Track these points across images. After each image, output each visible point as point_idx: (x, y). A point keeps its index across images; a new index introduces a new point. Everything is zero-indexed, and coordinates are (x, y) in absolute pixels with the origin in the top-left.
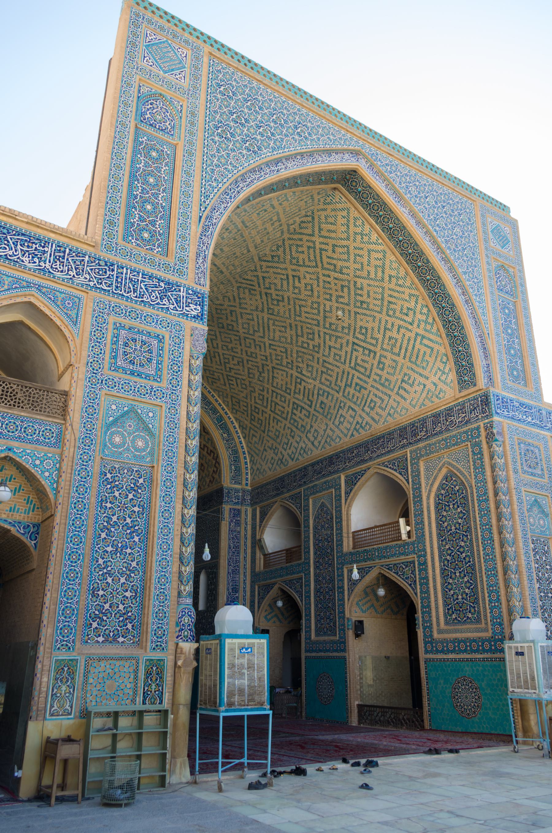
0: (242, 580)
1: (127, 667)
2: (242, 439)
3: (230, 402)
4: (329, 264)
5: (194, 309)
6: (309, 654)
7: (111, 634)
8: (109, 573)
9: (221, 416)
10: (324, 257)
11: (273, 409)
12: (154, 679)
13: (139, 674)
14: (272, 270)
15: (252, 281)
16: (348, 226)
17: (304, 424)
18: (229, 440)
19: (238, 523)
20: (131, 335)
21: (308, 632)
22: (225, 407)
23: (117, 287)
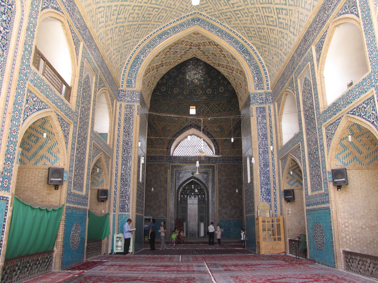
0: (270, 158)
2: (261, 57)
3: (245, 33)
6: (308, 208)
11: (267, 23)
17: (287, 22)
18: (250, 60)
19: (264, 117)
21: (306, 189)
22: (244, 38)
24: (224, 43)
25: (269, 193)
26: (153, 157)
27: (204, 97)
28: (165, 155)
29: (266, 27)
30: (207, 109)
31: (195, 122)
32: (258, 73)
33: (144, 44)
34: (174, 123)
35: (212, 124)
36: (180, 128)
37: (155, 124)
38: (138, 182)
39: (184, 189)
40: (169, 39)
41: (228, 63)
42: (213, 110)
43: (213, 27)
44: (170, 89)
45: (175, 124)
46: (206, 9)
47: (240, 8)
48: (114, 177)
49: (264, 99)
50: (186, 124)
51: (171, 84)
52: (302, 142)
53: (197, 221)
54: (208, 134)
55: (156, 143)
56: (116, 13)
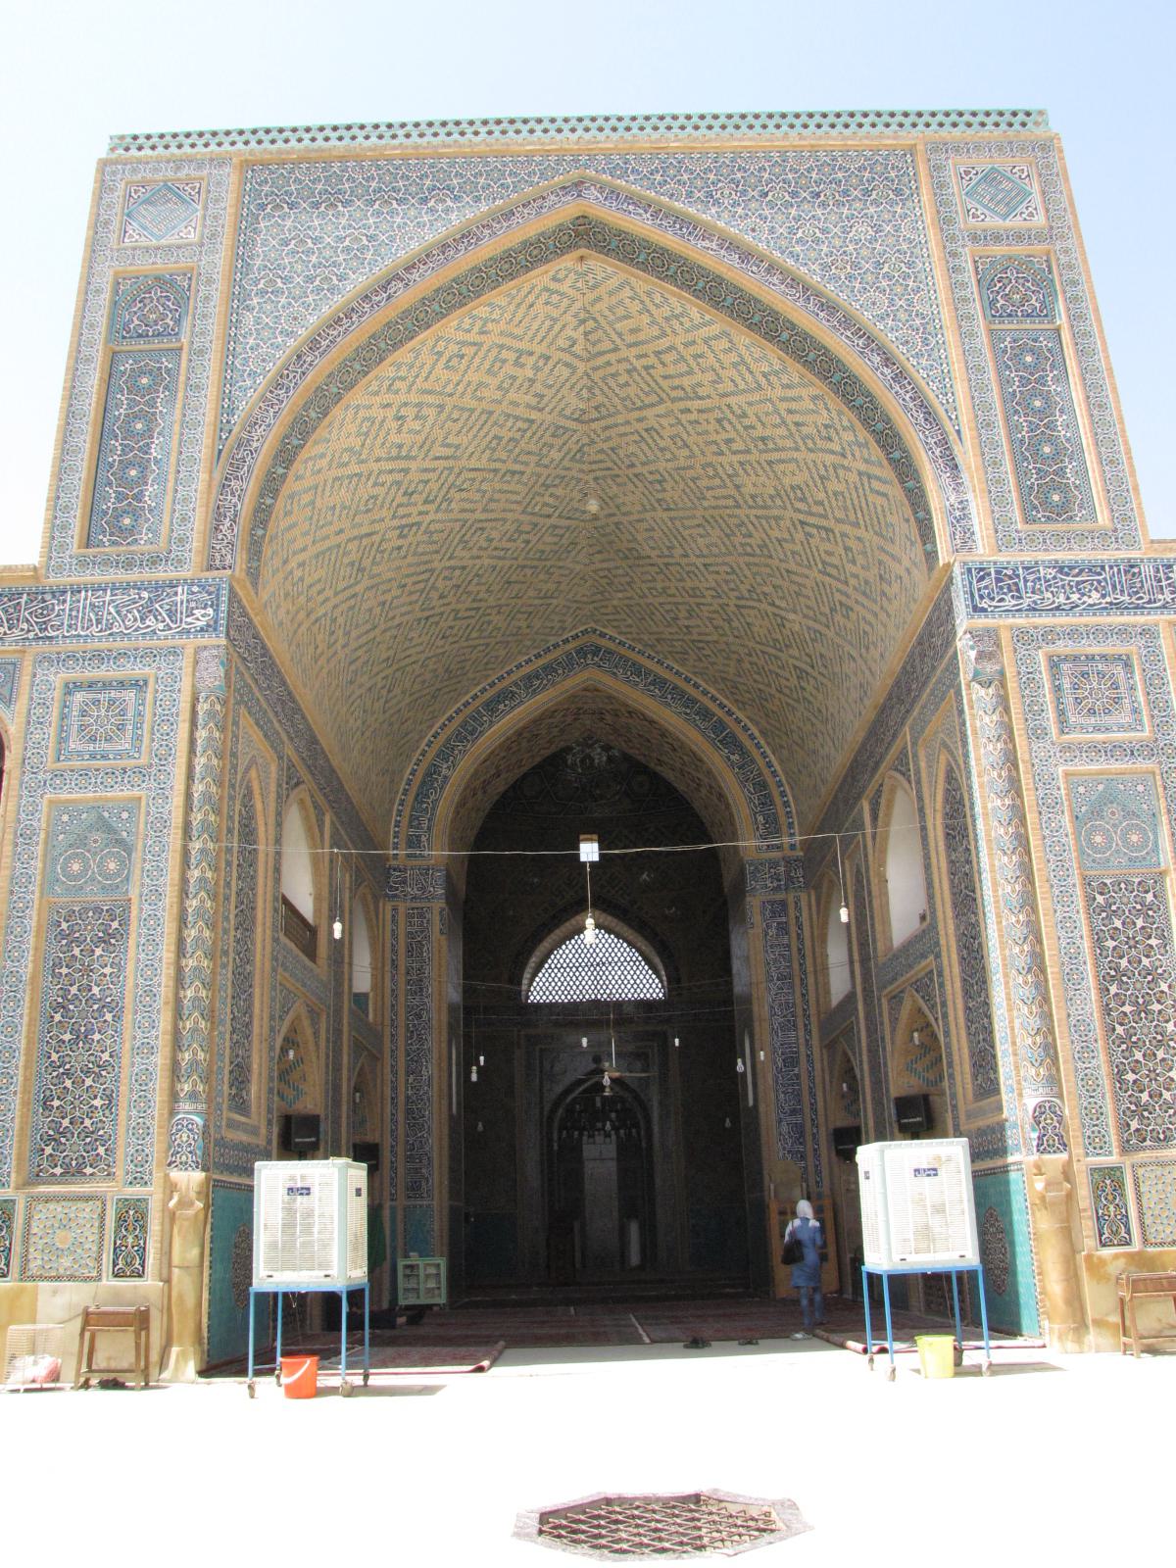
0: (802, 1041)
1: (89, 1210)
4: (674, 388)
5: (202, 617)
7: (74, 1163)
8: (67, 1073)
9: (720, 721)
10: (660, 380)
12: (131, 1228)
13: (107, 1222)
14: (613, 432)
15: (601, 461)
16: (648, 311)
18: (744, 764)
19: (783, 929)
20: (91, 696)
22: (725, 702)
23: (70, 626)
24: (670, 717)
25: (802, 1134)
29: (778, 695)
32: (766, 802)
33: (448, 731)
38: (451, 1116)
39: (570, 1110)
40: (516, 712)
41: (684, 764)
43: (638, 670)
46: (615, 624)
47: (709, 638)
48: (388, 1109)
49: (783, 877)
52: (857, 1018)
53: (615, 1214)
56: (384, 692)
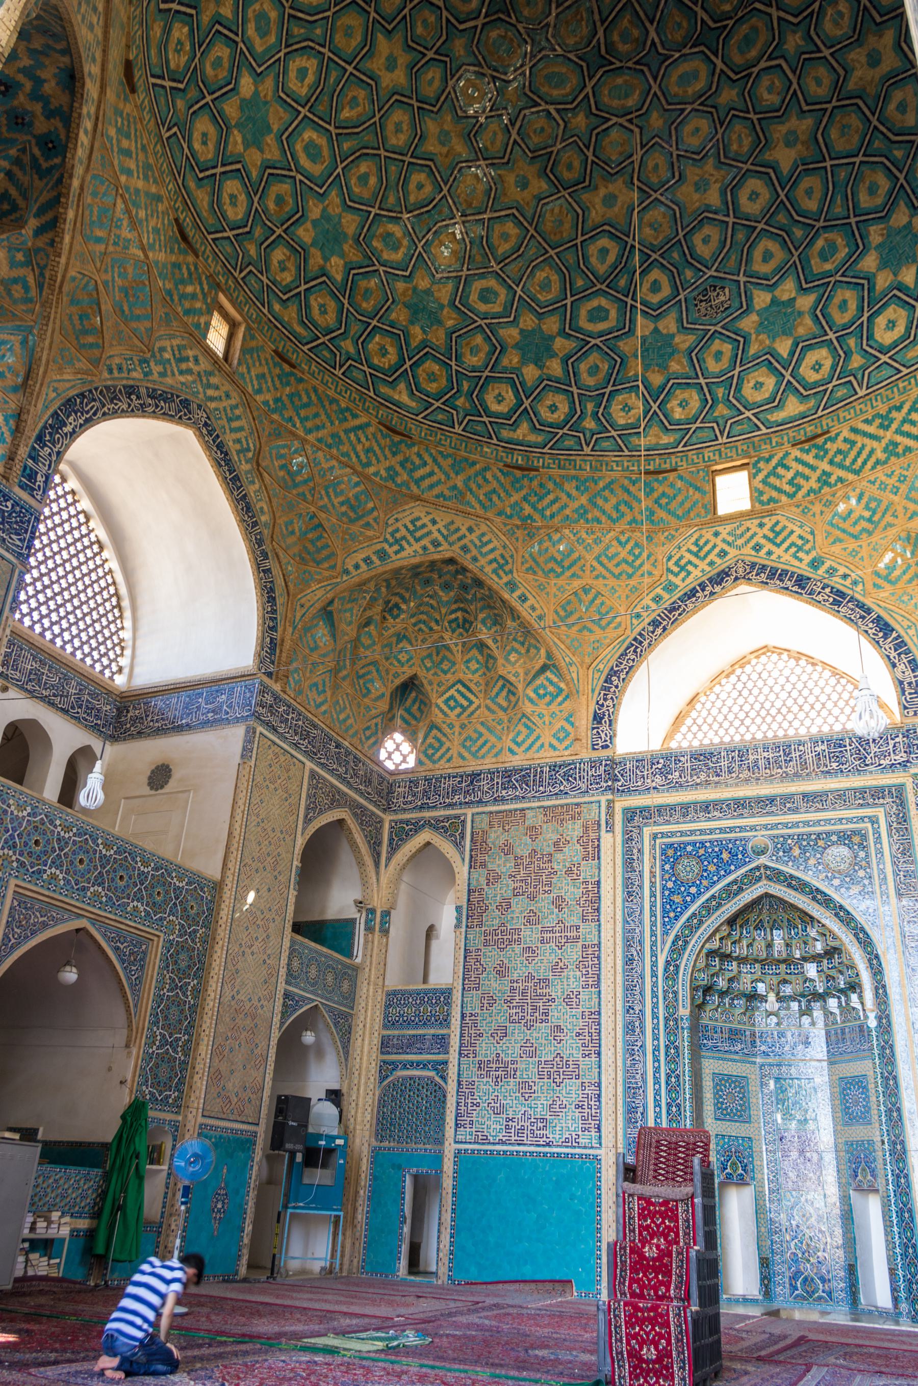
26: (517, 771)
27: (793, 407)
28: (586, 754)
30: (813, 468)
31: (748, 550)
34: (630, 576)
35: (855, 537)
36: (666, 596)
37: (512, 586)
42: (854, 461)
44: (590, 407)
45: (632, 582)
50: (696, 573)
51: (590, 381)
54: (836, 603)
55: (532, 695)
